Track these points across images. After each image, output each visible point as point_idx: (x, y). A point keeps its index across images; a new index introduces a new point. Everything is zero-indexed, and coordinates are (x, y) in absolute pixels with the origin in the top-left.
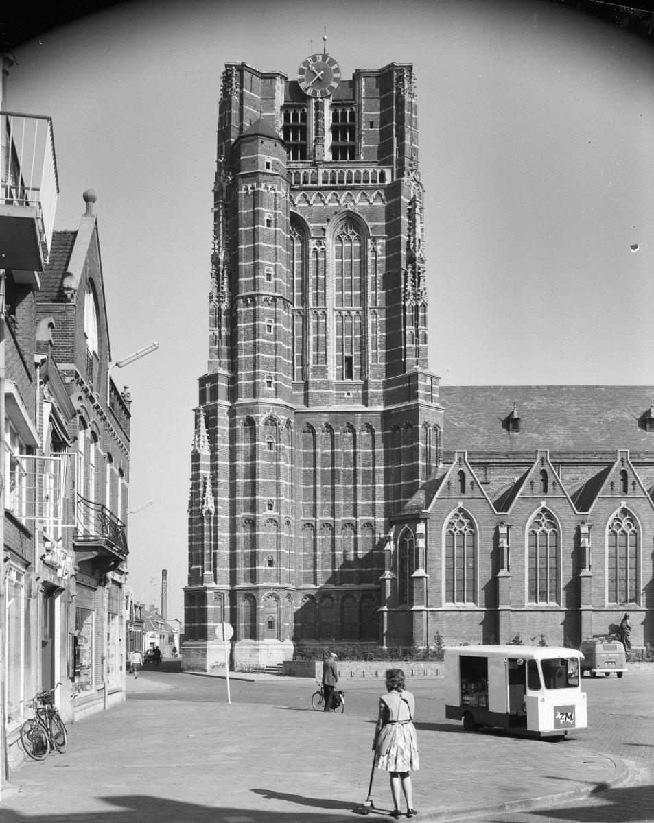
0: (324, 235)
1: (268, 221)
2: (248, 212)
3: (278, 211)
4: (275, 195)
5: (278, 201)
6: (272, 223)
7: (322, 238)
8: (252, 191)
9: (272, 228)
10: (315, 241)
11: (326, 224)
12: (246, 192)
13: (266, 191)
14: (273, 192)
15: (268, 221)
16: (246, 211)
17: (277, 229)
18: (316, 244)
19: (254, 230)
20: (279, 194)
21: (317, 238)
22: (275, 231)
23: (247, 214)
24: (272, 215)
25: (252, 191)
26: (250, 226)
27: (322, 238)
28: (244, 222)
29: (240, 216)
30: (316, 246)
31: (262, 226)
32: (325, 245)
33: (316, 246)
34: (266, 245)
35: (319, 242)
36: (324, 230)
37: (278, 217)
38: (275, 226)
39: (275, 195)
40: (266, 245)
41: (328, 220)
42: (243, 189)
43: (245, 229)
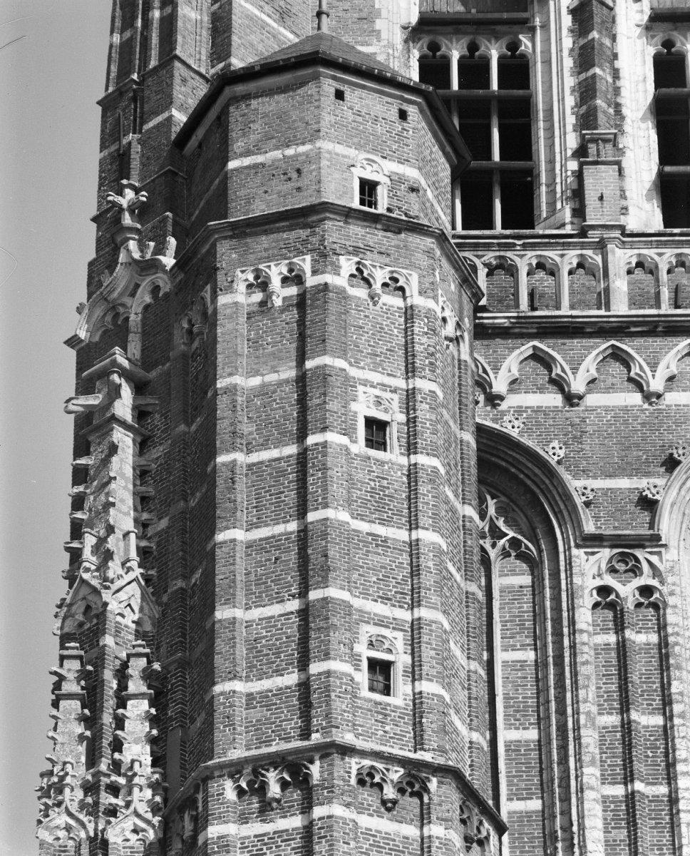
0: (651, 526)
1: (371, 423)
2: (263, 385)
3: (422, 384)
4: (410, 314)
5: (422, 343)
6: (394, 434)
7: (639, 542)
8: (293, 291)
9: (395, 456)
10: (606, 553)
11: (660, 482)
12: (258, 297)
13: (360, 292)
14: (396, 302)
15: (371, 423)
16: (256, 381)
17: (421, 459)
18: (613, 570)
19: (302, 460)
20: (429, 314)
21: (615, 541)
22: (412, 474)
23: (263, 391)
24: (396, 401)
25: (293, 291)
26: (279, 444)
27: (639, 542)
28: (247, 428)
29: (222, 403)
30: (609, 580)
31: (344, 440)
32: (656, 572)
33: (609, 580)
34: (364, 527)
35: (623, 558)
36: (649, 504)
37: (423, 411)
38: (411, 448)
39: (410, 314)
40: (364, 527)
41: (671, 464)
42: (242, 287)
43: (255, 458)
